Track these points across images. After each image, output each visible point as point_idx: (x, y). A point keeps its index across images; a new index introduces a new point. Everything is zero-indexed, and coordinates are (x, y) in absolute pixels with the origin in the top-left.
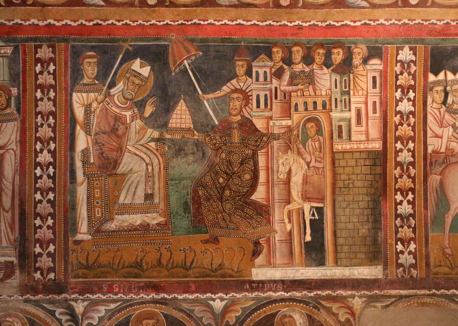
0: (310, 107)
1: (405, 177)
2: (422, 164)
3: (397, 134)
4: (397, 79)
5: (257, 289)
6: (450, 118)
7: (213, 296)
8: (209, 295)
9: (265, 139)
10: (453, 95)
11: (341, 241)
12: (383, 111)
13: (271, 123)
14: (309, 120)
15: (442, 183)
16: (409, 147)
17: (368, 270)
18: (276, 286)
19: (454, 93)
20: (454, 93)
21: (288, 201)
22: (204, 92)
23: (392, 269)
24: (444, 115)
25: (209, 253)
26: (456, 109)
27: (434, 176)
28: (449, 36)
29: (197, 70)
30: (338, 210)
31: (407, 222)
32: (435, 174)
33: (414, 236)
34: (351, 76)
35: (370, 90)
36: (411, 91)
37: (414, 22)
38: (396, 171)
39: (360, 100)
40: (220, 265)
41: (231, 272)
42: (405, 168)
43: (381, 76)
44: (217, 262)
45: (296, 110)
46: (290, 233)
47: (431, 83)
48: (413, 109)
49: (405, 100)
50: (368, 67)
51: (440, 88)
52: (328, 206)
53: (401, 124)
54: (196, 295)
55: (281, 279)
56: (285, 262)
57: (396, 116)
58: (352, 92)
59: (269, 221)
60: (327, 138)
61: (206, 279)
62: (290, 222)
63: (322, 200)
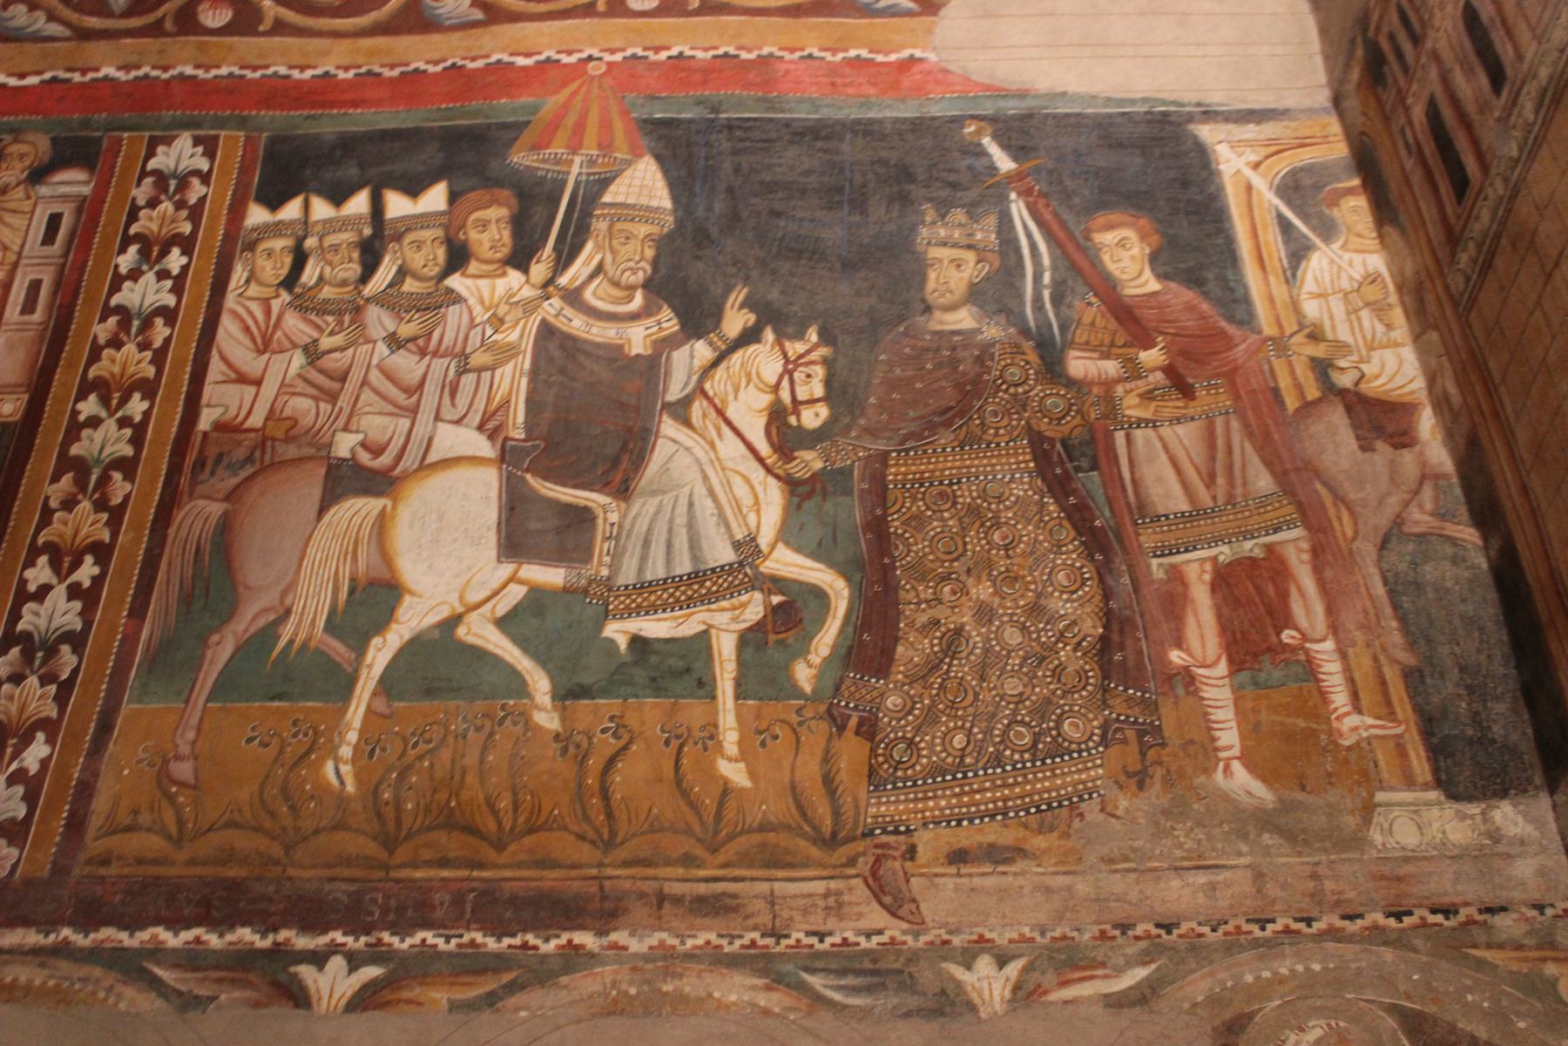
1: (86, 505)
2: (165, 467)
3: (92, 373)
4: (133, 216)
6: (302, 326)
10: (324, 259)
15: (225, 528)
16: (128, 413)
19: (329, 256)
20: (329, 256)
26: (326, 301)
27: (201, 503)
28: (331, 107)
31: (44, 662)
32: (209, 497)
33: (54, 714)
35: (32, 248)
36: (176, 251)
37: (214, 72)
38: (55, 486)
42: (94, 478)
43: (79, 211)
47: (254, 230)
48: (171, 301)
49: (149, 277)
50: (44, 190)
51: (278, 244)
53: (116, 343)
57: (103, 319)
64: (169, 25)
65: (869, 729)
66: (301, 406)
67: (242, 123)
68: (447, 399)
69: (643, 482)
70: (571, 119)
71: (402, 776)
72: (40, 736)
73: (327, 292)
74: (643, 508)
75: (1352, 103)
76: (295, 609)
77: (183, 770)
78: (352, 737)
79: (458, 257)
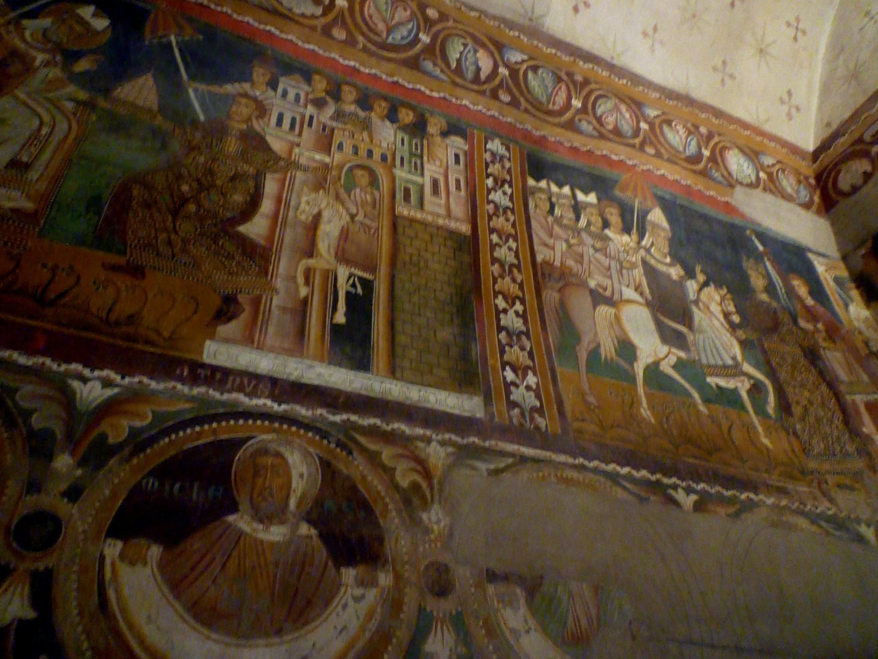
0: (363, 152)
5: (209, 381)
7: (87, 372)
8: (76, 367)
9: (282, 163)
11: (402, 339)
12: (470, 193)
13: (297, 150)
14: (359, 166)
17: (456, 400)
18: (256, 386)
21: (310, 251)
22: (192, 77)
23: (499, 407)
24: (552, 225)
25: (111, 290)
29: (188, 51)
30: (398, 292)
33: (531, 364)
34: (425, 142)
39: (438, 170)
40: (131, 317)
41: (153, 336)
44: (126, 308)
45: (340, 147)
46: (305, 303)
51: (543, 196)
52: (381, 280)
54: (40, 360)
55: (270, 374)
56: (286, 346)
58: (425, 158)
59: (264, 271)
60: (385, 195)
61: (85, 334)
62: (307, 283)
63: (373, 269)
64: (488, 93)
65: (795, 434)
66: (570, 263)
67: (516, 143)
68: (620, 275)
69: (696, 327)
70: (632, 184)
71: (667, 419)
72: (530, 373)
73: (565, 221)
74: (700, 337)
75: (858, 261)
76: (602, 342)
77: (591, 399)
78: (644, 400)
79: (606, 224)
